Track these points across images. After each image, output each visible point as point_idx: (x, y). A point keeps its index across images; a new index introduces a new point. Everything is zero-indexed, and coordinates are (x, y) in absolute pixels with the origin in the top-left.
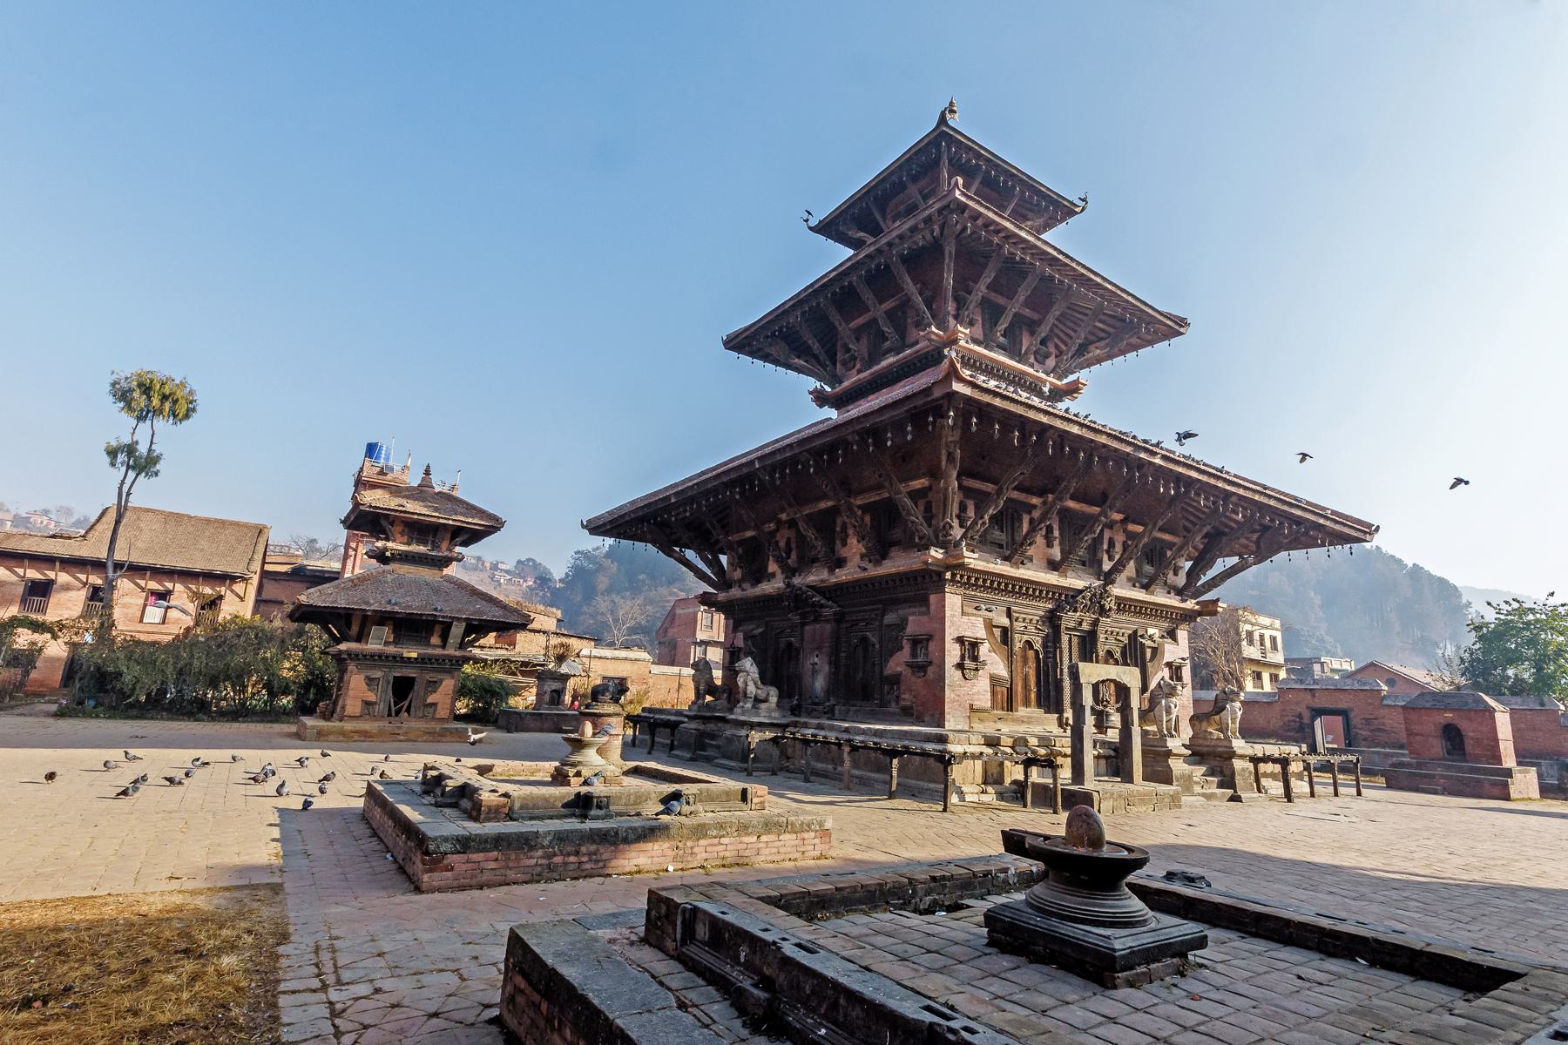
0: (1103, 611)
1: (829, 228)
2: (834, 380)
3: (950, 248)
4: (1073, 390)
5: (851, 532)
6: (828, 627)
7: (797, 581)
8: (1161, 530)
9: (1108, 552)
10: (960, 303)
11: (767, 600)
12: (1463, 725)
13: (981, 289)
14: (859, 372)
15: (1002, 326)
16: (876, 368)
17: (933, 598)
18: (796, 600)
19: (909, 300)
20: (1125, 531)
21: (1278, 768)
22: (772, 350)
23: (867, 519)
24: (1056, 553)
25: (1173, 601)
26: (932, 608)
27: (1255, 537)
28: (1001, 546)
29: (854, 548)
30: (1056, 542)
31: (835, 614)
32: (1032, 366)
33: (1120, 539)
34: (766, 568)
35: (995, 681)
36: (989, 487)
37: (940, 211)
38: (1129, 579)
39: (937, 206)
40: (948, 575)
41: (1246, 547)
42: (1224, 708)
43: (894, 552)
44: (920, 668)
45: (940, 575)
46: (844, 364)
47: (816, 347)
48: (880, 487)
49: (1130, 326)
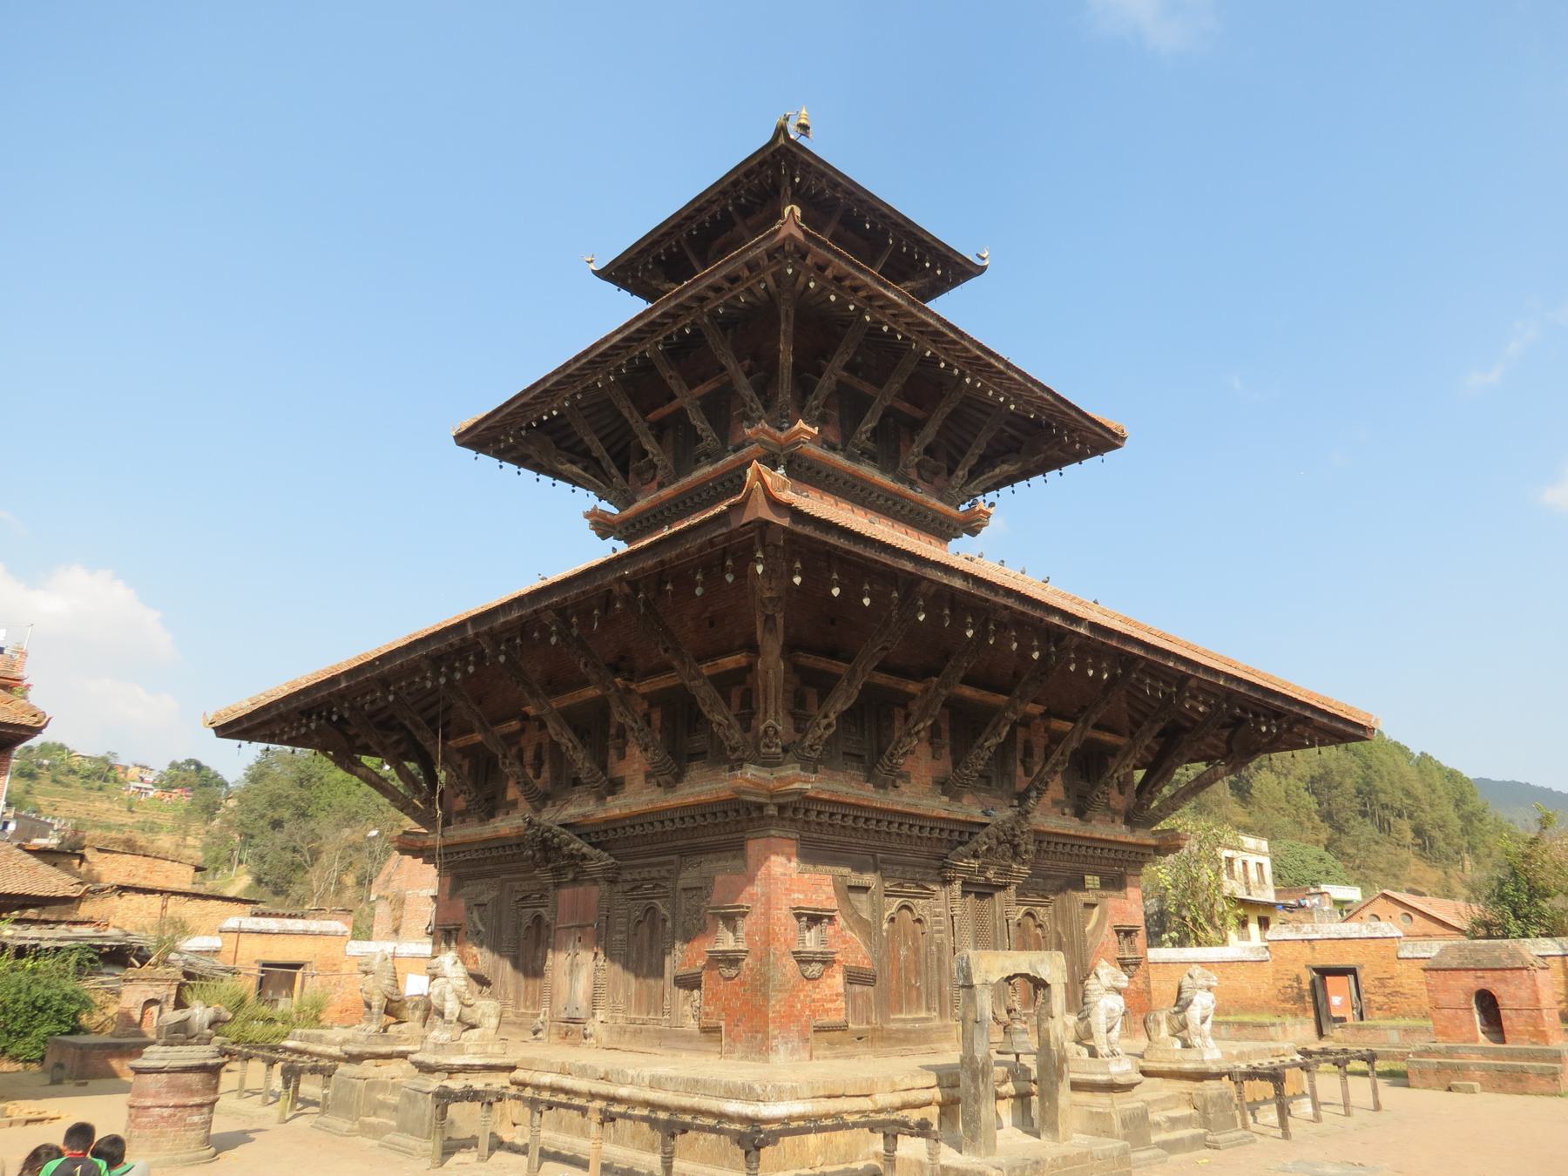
0: (1016, 854)
1: (622, 272)
2: (623, 501)
3: (786, 309)
4: (972, 526)
5: (629, 735)
6: (596, 888)
7: (551, 816)
8: (1097, 727)
9: (1023, 762)
10: (803, 387)
11: (501, 843)
12: (1498, 990)
13: (834, 372)
14: (661, 486)
15: (868, 425)
16: (685, 481)
17: (753, 847)
18: (545, 852)
19: (730, 383)
20: (1047, 729)
21: (1267, 1088)
22: (531, 450)
23: (656, 717)
24: (945, 764)
25: (1120, 832)
26: (751, 862)
27: (1226, 733)
28: (859, 757)
29: (634, 763)
30: (946, 751)
31: (606, 870)
32: (912, 484)
33: (1040, 741)
34: (505, 790)
35: (855, 977)
36: (839, 667)
37: (770, 255)
38: (1056, 803)
39: (764, 246)
40: (772, 811)
41: (1215, 747)
42: (1189, 1003)
43: (695, 771)
46: (639, 474)
47: (598, 449)
48: (667, 668)
49: (1047, 435)
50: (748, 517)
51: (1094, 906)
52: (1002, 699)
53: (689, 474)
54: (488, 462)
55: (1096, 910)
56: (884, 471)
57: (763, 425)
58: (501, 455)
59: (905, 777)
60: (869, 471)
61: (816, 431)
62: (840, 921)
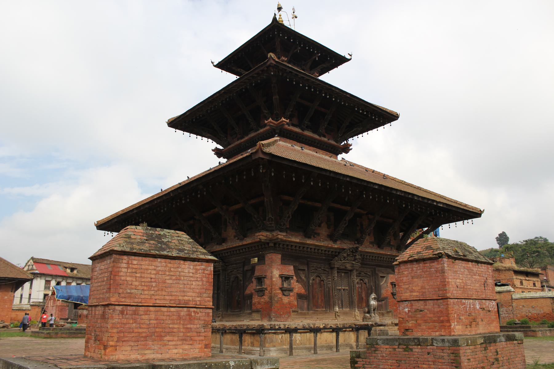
1: (225, 65)
4: (346, 149)
16: (246, 138)
29: (231, 232)
32: (324, 136)
40: (272, 245)
44: (261, 292)
45: (268, 244)
50: (257, 157)
51: (384, 277)
52: (348, 208)
53: (247, 135)
54: (180, 132)
55: (385, 279)
56: (315, 132)
57: (270, 119)
58: (184, 130)
59: (318, 234)
60: (308, 133)
61: (288, 121)
62: (295, 278)
